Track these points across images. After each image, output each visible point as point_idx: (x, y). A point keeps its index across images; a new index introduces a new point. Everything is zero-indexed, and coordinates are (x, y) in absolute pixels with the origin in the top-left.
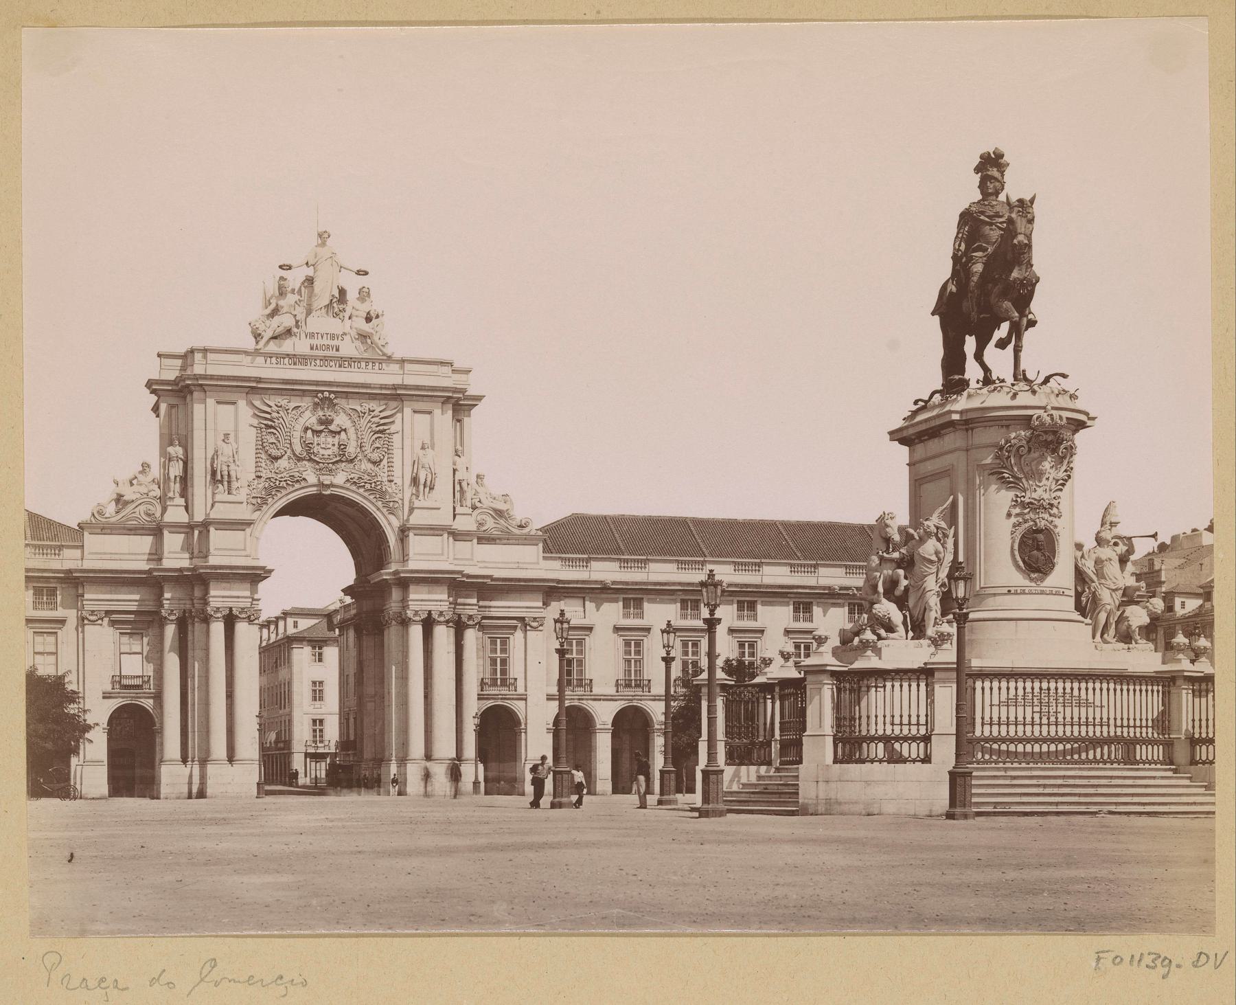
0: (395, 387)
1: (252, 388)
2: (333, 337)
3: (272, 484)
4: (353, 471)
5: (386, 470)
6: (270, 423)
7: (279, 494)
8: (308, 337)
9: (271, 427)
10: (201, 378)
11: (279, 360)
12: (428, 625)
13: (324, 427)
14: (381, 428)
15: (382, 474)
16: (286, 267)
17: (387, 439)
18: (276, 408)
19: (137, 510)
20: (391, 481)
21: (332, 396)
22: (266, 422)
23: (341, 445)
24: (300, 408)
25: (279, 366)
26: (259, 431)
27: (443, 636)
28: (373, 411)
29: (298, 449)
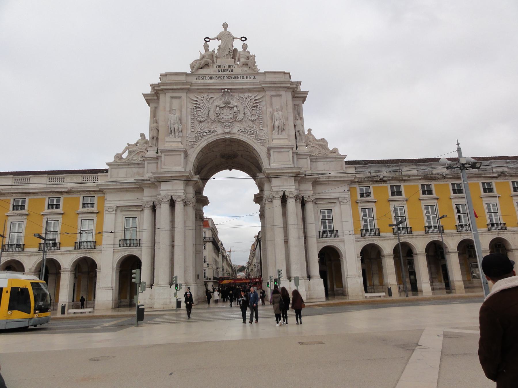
1: (189, 90)
2: (230, 66)
3: (199, 135)
4: (242, 126)
6: (198, 106)
7: (203, 139)
8: (218, 67)
9: (199, 108)
11: (203, 78)
12: (284, 200)
14: (255, 104)
16: (207, 40)
17: (258, 110)
18: (201, 99)
19: (136, 156)
20: (262, 130)
22: (196, 106)
23: (234, 113)
24: (213, 98)
25: (202, 80)
27: (292, 205)
28: (251, 97)
29: (213, 117)
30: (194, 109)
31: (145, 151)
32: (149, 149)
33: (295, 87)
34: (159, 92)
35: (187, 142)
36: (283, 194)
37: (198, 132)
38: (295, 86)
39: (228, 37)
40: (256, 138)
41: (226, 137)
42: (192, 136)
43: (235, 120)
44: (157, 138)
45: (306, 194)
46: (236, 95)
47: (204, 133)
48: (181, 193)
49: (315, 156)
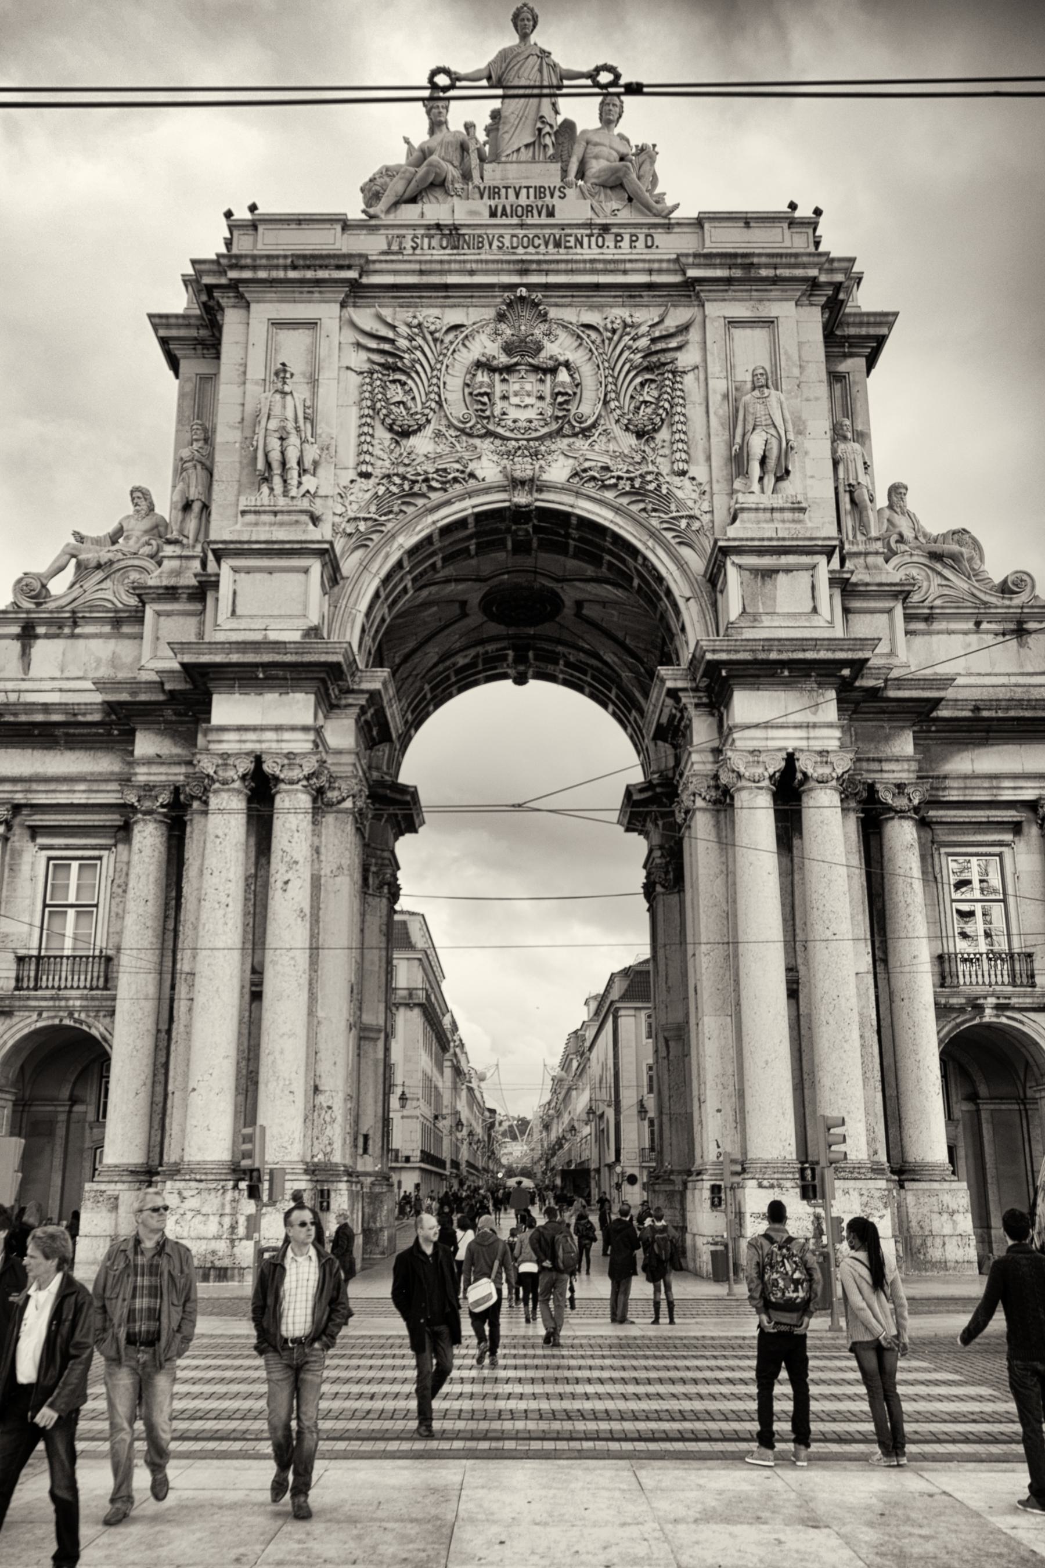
0: (679, 263)
4: (590, 455)
5: (666, 451)
6: (390, 360)
7: (410, 510)
10: (232, 267)
13: (515, 360)
14: (654, 359)
15: (659, 460)
17: (667, 382)
20: (683, 473)
21: (537, 296)
22: (382, 361)
23: (559, 393)
25: (418, 252)
26: (368, 380)
30: (375, 376)
31: (150, 564)
32: (169, 550)
33: (838, 287)
34: (225, 300)
35: (337, 519)
36: (783, 764)
37: (388, 476)
38: (839, 277)
39: (536, 67)
40: (655, 510)
41: (516, 500)
42: (360, 495)
43: (561, 428)
44: (206, 507)
45: (885, 775)
46: (569, 315)
47: (417, 481)
48: (301, 743)
49: (926, 604)
